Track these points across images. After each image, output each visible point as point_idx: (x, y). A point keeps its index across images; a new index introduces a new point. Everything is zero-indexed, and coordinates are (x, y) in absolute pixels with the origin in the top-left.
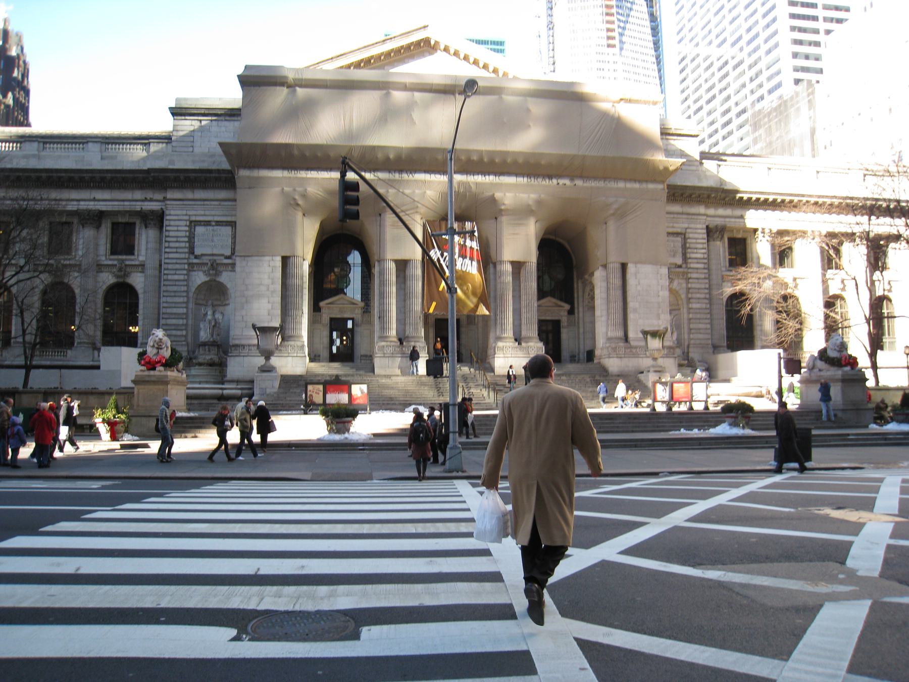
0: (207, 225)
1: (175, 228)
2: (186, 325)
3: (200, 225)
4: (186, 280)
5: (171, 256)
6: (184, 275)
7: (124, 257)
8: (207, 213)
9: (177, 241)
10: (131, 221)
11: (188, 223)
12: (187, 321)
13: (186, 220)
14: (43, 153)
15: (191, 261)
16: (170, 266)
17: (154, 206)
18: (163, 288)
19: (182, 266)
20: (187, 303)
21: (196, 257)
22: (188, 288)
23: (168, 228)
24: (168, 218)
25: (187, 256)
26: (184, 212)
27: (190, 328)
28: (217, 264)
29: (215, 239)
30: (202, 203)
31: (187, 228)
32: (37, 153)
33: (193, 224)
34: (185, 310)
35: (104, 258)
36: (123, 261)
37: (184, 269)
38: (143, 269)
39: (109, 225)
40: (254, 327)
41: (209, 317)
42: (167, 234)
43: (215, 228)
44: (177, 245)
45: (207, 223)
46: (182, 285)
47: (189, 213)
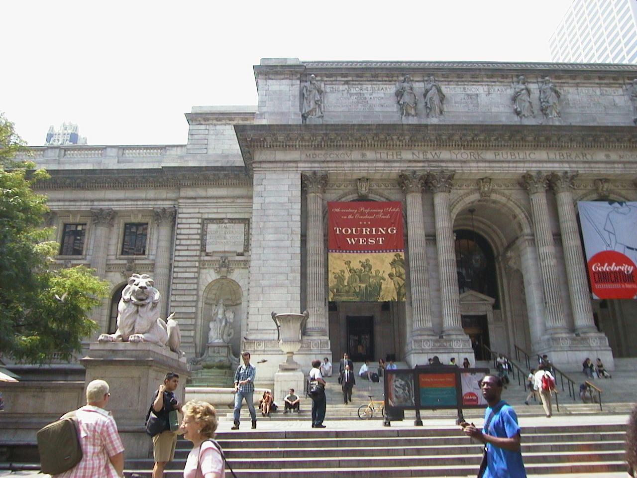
0: (220, 223)
1: (187, 226)
2: (195, 325)
3: (213, 223)
4: (197, 278)
5: (182, 253)
6: (195, 272)
7: (135, 257)
8: (219, 210)
9: (188, 239)
10: (144, 221)
11: (200, 221)
12: (196, 322)
13: (198, 218)
14: (62, 159)
15: (202, 258)
16: (180, 264)
17: (167, 204)
18: (173, 287)
19: (193, 264)
20: (197, 301)
21: (207, 255)
22: (198, 287)
23: (179, 226)
24: (180, 216)
25: (198, 253)
26: (197, 210)
27: (198, 328)
28: (229, 261)
29: (228, 236)
30: (215, 201)
31: (199, 226)
32: (58, 158)
33: (205, 222)
34: (194, 310)
35: (113, 257)
36: (133, 260)
37: (195, 267)
38: (152, 268)
39: (122, 226)
40: (274, 316)
41: (220, 316)
42: (178, 231)
43: (228, 225)
44: (188, 242)
45: (221, 221)
46: (192, 283)
47: (201, 211)
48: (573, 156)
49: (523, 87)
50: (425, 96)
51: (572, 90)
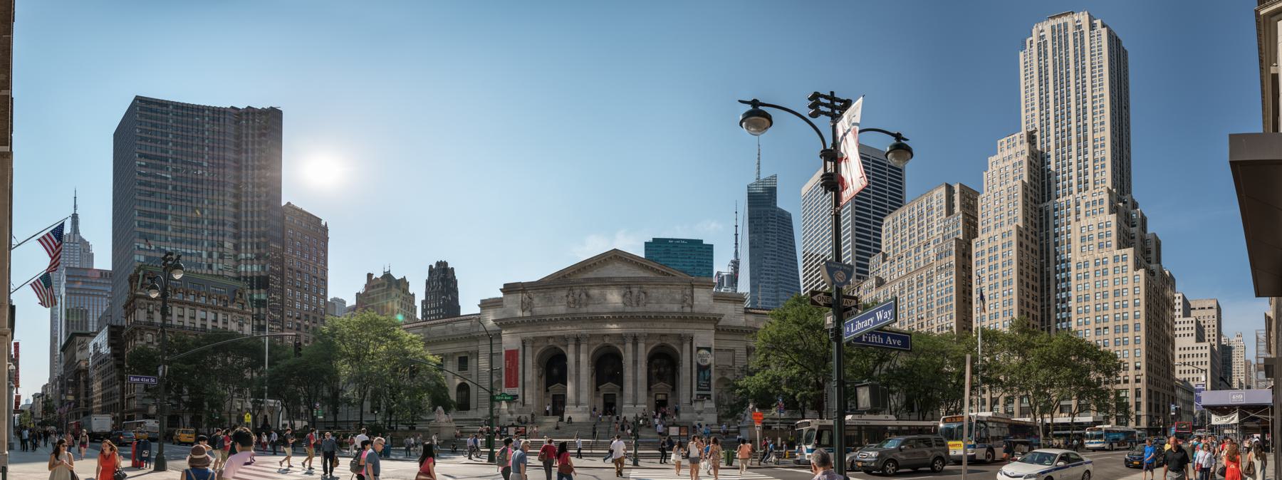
48: (647, 324)
49: (628, 290)
50: (580, 296)
51: (654, 290)
